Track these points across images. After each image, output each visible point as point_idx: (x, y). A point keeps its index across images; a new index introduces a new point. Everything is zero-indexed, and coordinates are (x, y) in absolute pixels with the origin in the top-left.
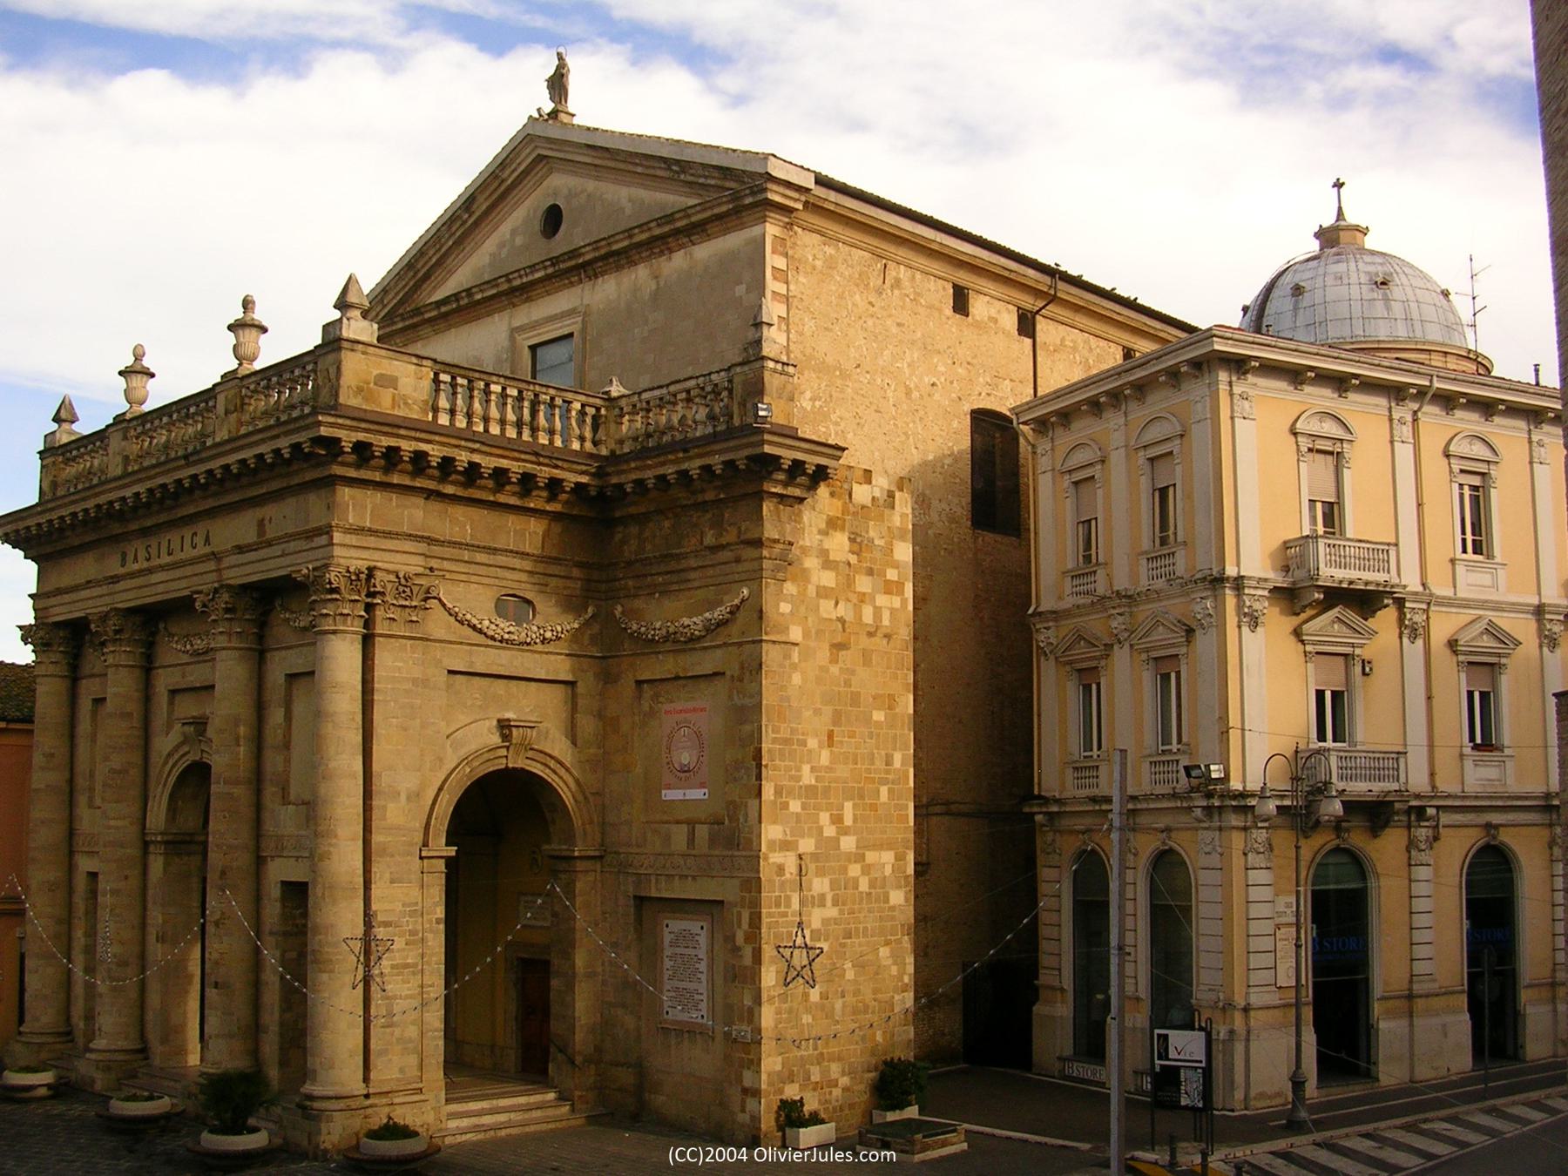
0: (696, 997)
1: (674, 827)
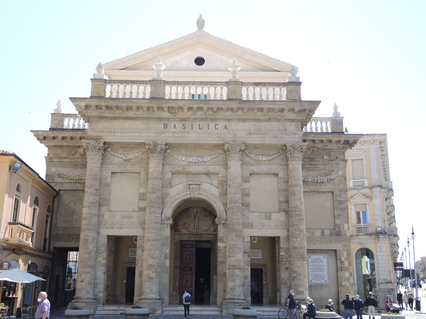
0: (323, 276)
1: (316, 231)
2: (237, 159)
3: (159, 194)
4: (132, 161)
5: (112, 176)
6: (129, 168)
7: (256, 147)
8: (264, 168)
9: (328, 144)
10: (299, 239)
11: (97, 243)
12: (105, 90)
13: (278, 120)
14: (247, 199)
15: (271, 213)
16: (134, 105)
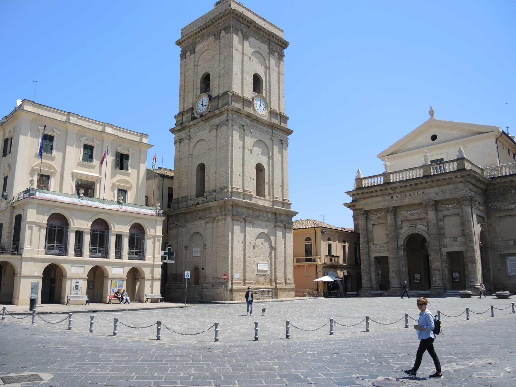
1: (510, 241)
2: (432, 210)
3: (393, 234)
4: (381, 217)
5: (372, 227)
6: (380, 221)
7: (445, 200)
8: (451, 212)
9: (512, 183)
10: (470, 252)
11: (369, 261)
12: (362, 183)
13: (453, 183)
14: (443, 231)
15: (457, 237)
16: (373, 190)
